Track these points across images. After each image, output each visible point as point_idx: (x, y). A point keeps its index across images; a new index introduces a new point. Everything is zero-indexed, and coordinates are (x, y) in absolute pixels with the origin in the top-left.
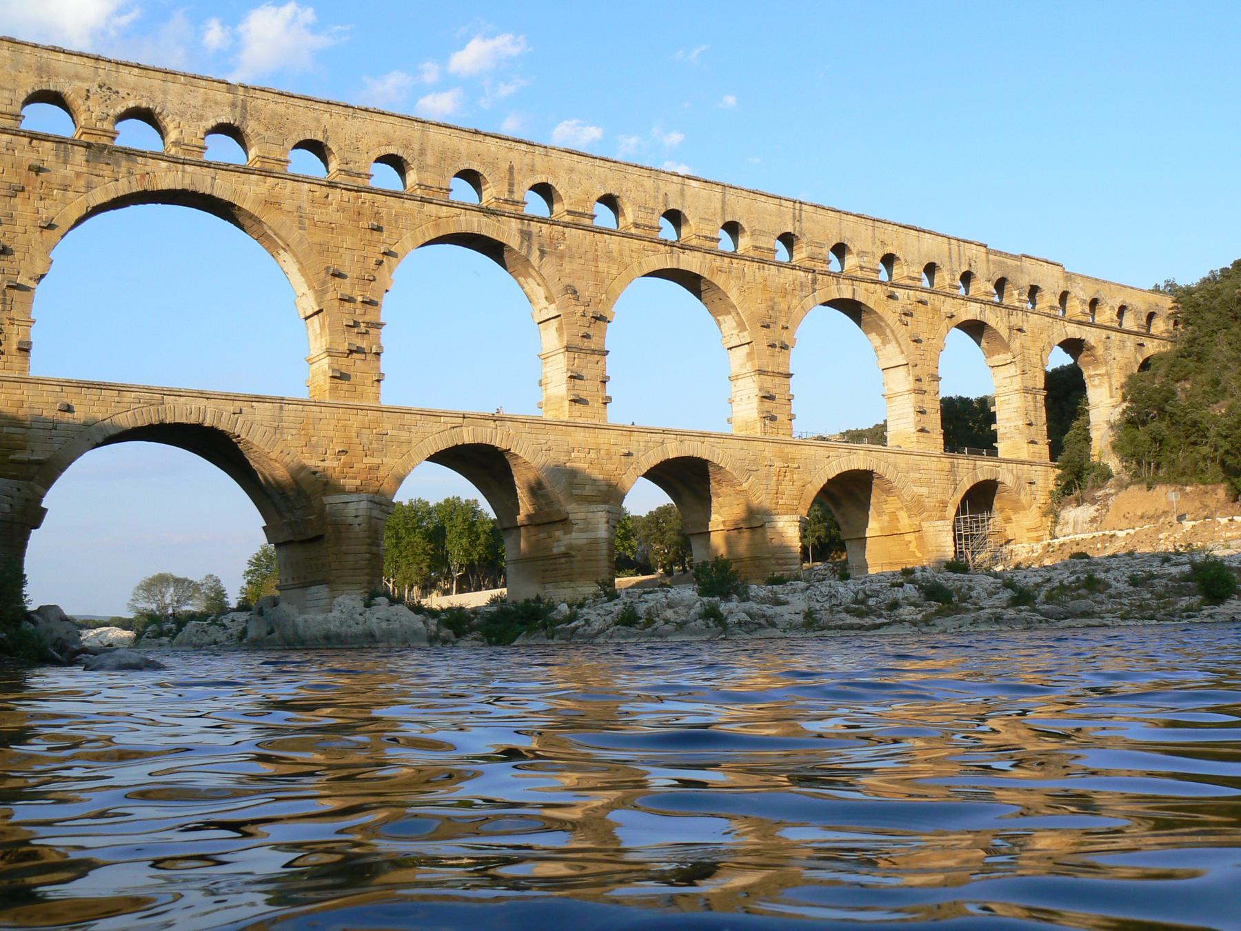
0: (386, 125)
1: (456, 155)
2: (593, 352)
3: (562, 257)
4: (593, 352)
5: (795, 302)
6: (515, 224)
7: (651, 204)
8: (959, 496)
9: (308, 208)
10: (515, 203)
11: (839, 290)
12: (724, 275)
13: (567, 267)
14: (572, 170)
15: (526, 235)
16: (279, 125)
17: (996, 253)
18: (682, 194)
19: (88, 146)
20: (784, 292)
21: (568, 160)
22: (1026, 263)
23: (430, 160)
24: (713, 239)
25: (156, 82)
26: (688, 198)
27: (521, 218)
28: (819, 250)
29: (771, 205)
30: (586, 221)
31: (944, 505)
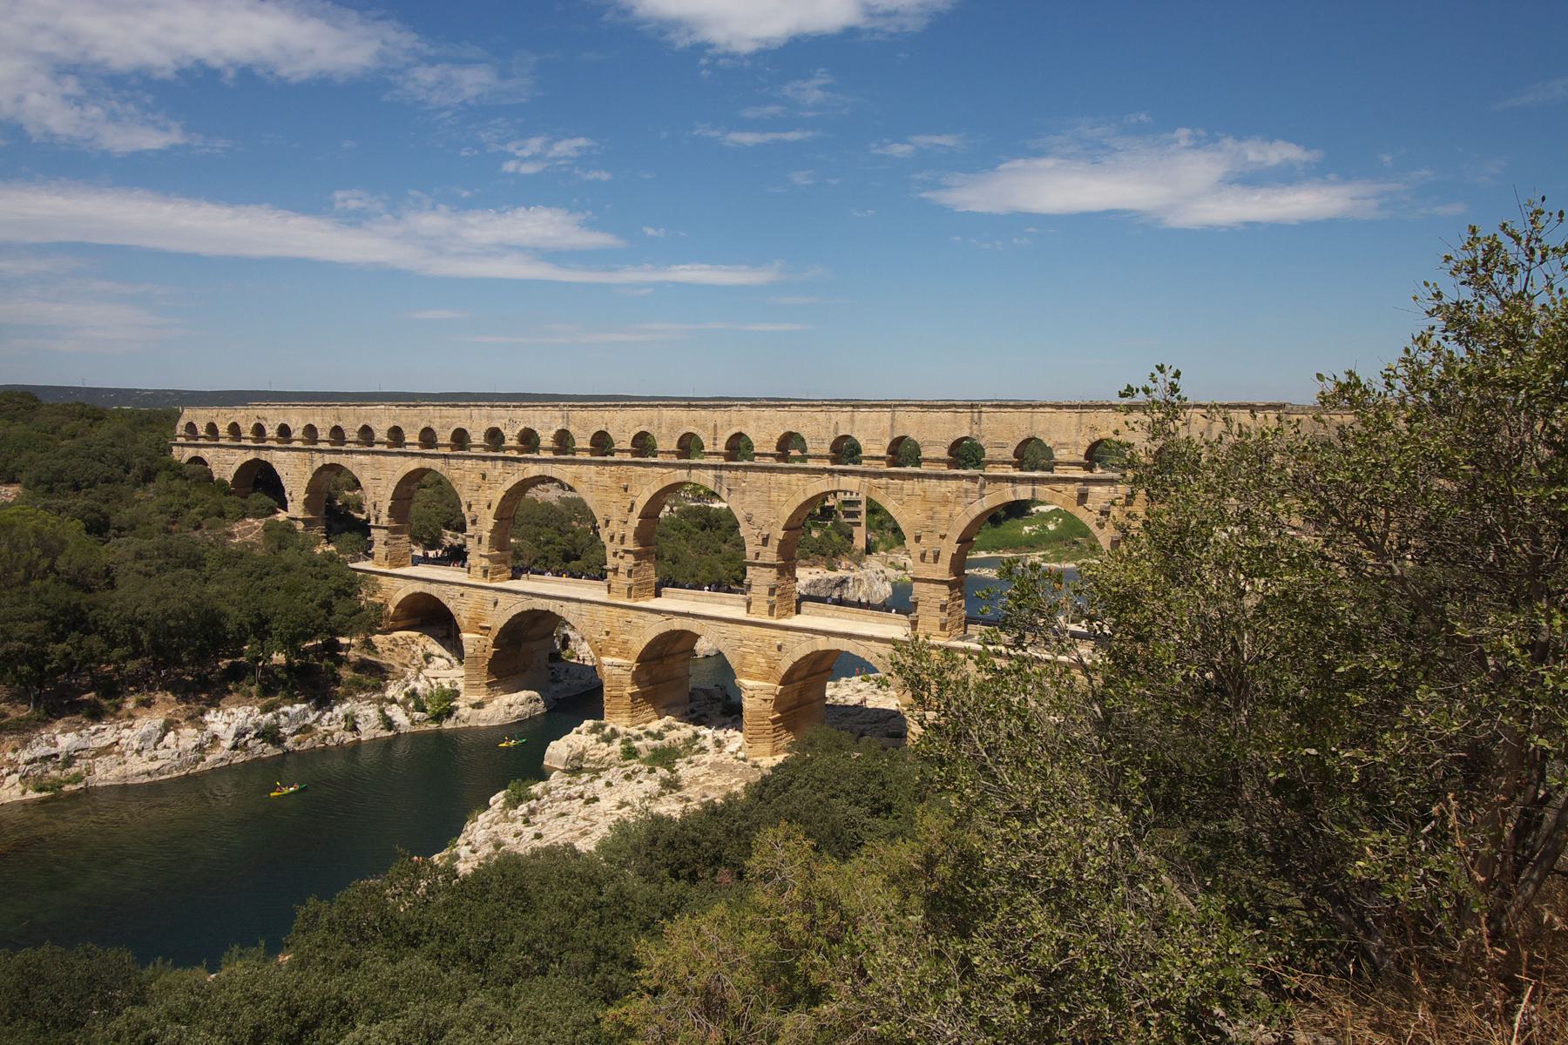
2: (765, 565)
3: (744, 492)
4: (765, 565)
5: (959, 509)
6: (711, 472)
7: (823, 434)
9: (595, 478)
11: (1014, 492)
12: (882, 492)
13: (747, 499)
14: (759, 418)
15: (719, 478)
16: (584, 426)
18: (852, 420)
20: (945, 501)
23: (664, 431)
24: (878, 458)
26: (857, 423)
28: (1000, 451)
29: (946, 415)
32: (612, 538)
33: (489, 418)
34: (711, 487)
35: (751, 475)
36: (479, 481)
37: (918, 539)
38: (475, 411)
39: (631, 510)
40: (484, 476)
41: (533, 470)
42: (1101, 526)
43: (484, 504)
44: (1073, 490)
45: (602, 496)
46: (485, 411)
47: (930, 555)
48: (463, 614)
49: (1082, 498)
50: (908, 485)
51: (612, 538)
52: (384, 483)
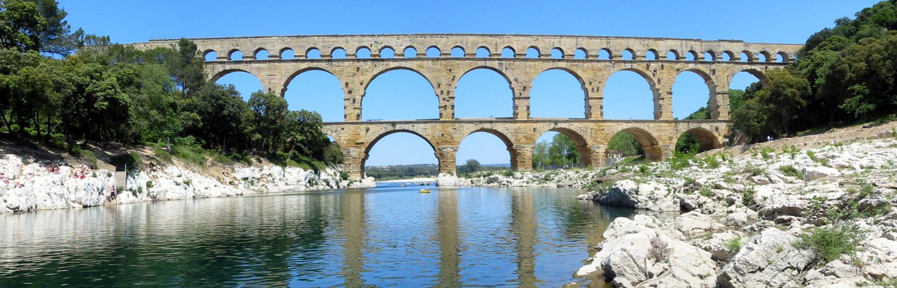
0: (455, 38)
1: (478, 42)
2: (525, 98)
4: (525, 98)
6: (497, 62)
8: (679, 135)
10: (498, 55)
15: (500, 64)
17: (706, 42)
18: (560, 42)
19: (371, 60)
20: (600, 70)
21: (516, 38)
22: (722, 43)
25: (388, 38)
27: (499, 59)
30: (523, 57)
31: (671, 138)
32: (442, 92)
33: (359, 41)
34: (497, 67)
35: (517, 63)
36: (355, 72)
37: (590, 83)
38: (349, 38)
39: (453, 80)
40: (358, 69)
41: (393, 64)
42: (654, 75)
43: (357, 83)
44: (645, 64)
45: (437, 74)
46: (356, 38)
47: (595, 89)
48: (342, 139)
49: (648, 66)
50: (586, 64)
51: (442, 92)
52: (279, 77)
